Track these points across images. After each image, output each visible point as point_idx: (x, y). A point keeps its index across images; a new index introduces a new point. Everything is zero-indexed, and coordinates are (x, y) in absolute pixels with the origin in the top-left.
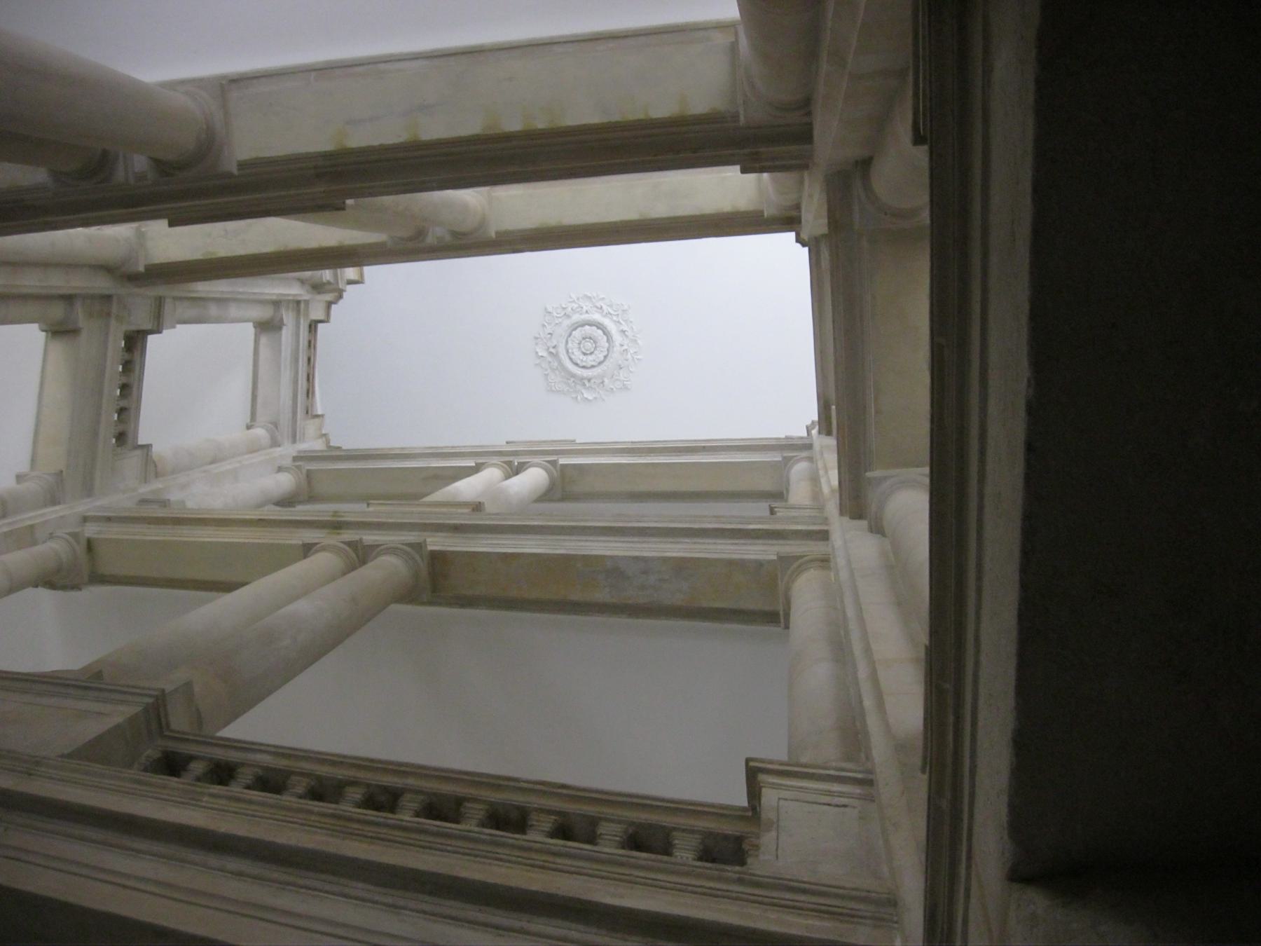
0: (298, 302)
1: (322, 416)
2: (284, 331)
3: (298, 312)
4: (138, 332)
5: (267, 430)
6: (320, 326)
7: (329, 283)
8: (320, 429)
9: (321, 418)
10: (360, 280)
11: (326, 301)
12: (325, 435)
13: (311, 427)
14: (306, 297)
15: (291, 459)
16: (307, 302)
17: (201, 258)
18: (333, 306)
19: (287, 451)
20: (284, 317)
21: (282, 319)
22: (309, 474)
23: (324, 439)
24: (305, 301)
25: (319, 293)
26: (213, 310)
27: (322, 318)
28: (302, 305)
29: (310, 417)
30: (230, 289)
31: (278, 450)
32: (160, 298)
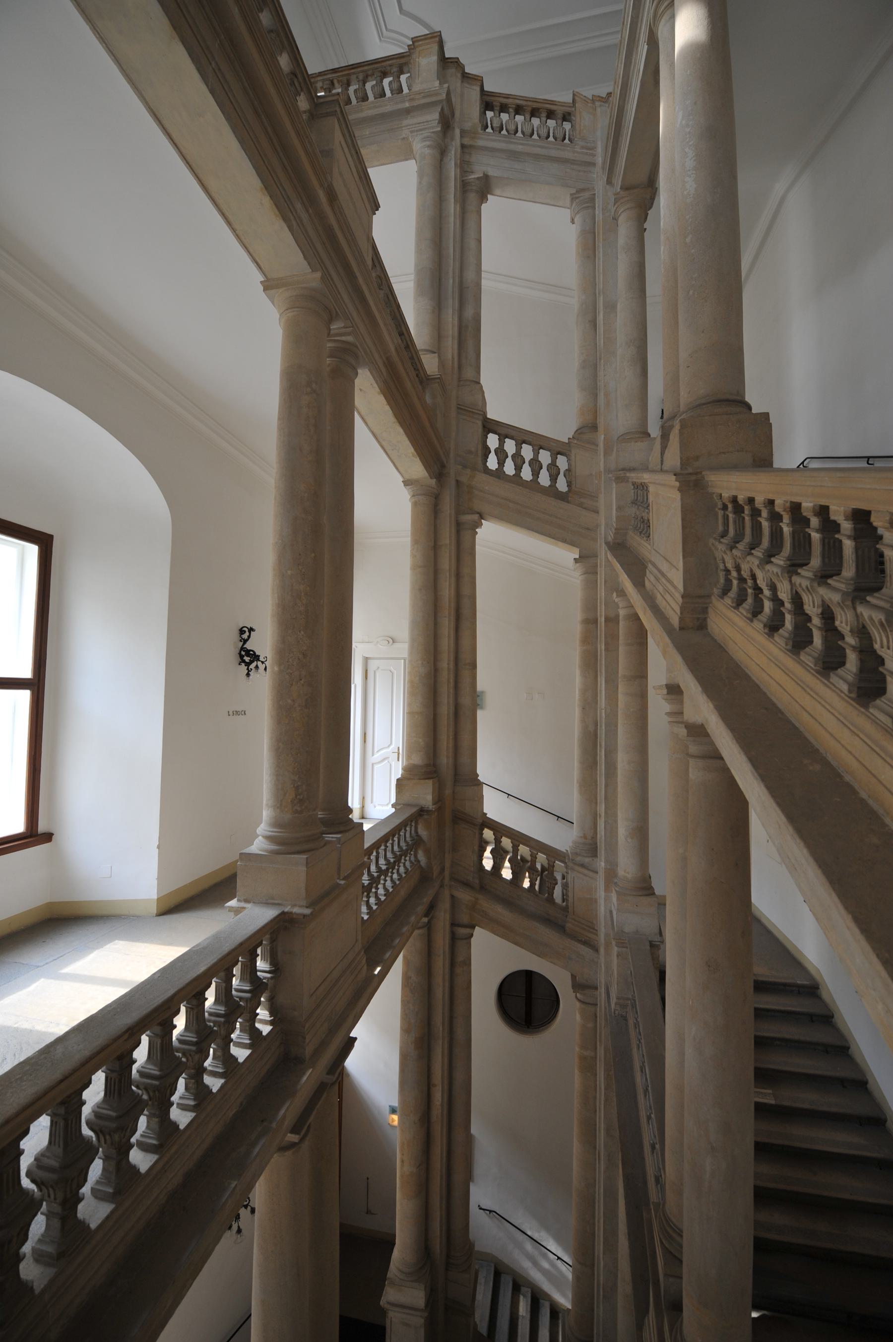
0: (463, 146)
1: (574, 95)
2: (492, 172)
3: (471, 146)
4: (484, 426)
5: (578, 212)
6: (486, 89)
7: (442, 113)
8: (585, 100)
9: (576, 98)
10: (437, 39)
11: (462, 82)
12: (593, 101)
13: (583, 118)
14: (457, 132)
15: (608, 187)
16: (463, 133)
17: (418, 458)
18: (467, 71)
19: (600, 185)
20: (476, 176)
21: (478, 178)
22: (625, 188)
23: (598, 104)
24: (462, 137)
25: (453, 115)
26: (469, 312)
27: (478, 89)
28: (466, 141)
29: (573, 109)
30: (450, 301)
31: (599, 202)
32: (458, 408)
